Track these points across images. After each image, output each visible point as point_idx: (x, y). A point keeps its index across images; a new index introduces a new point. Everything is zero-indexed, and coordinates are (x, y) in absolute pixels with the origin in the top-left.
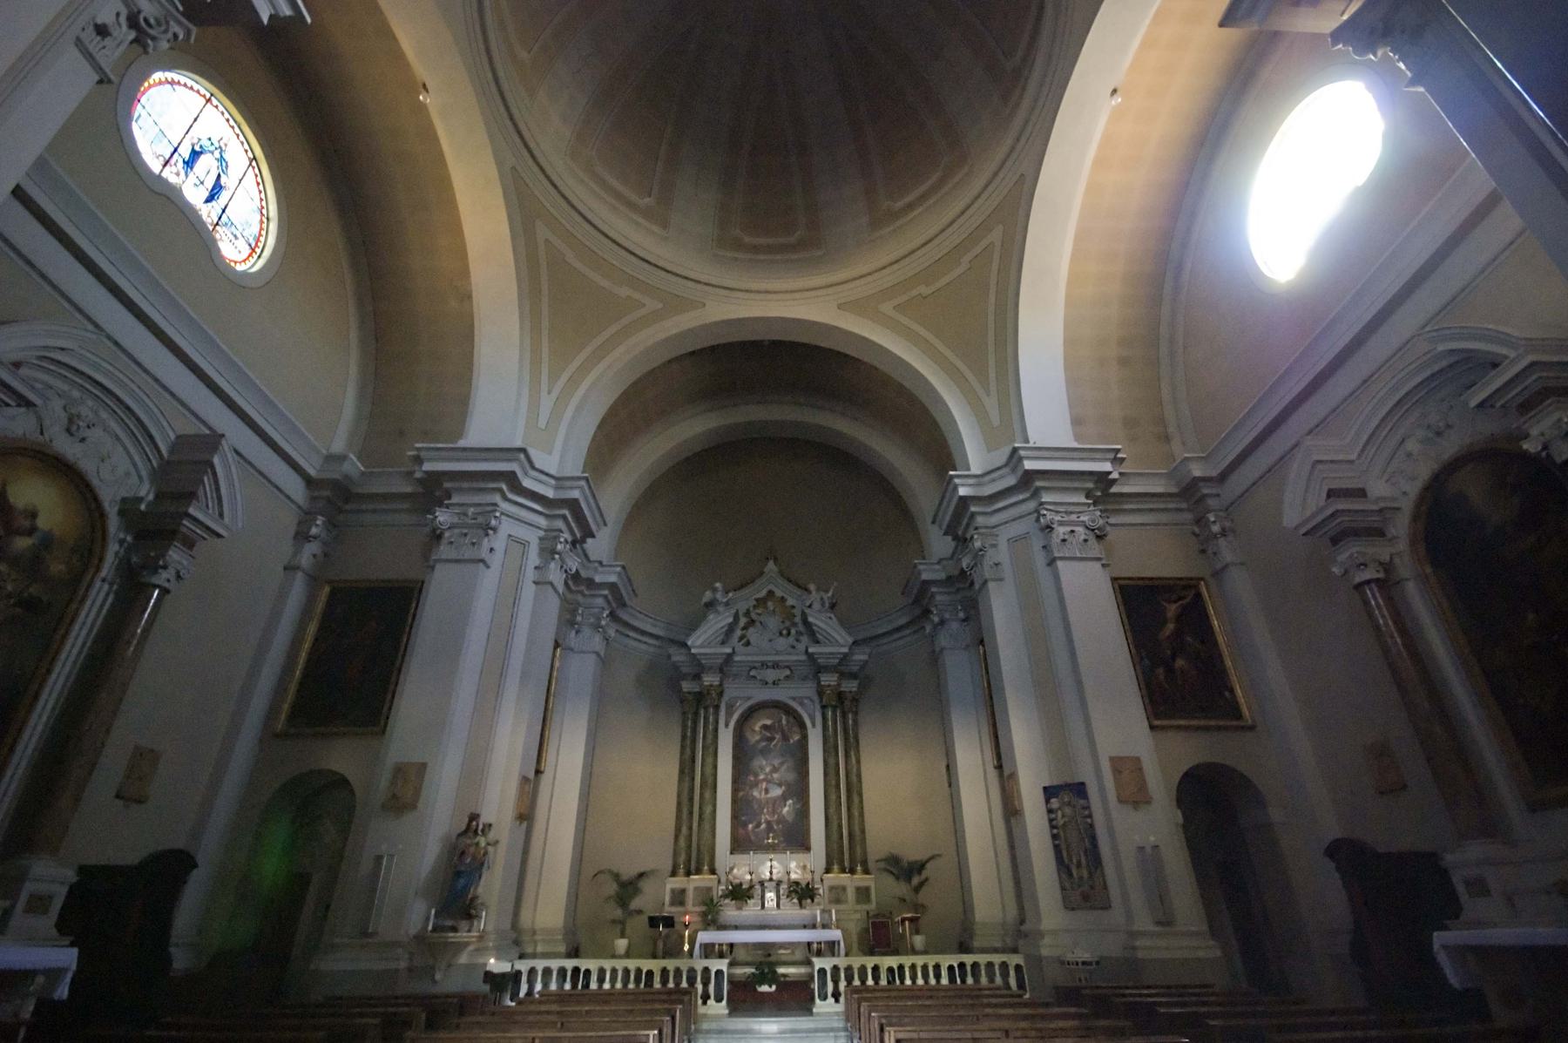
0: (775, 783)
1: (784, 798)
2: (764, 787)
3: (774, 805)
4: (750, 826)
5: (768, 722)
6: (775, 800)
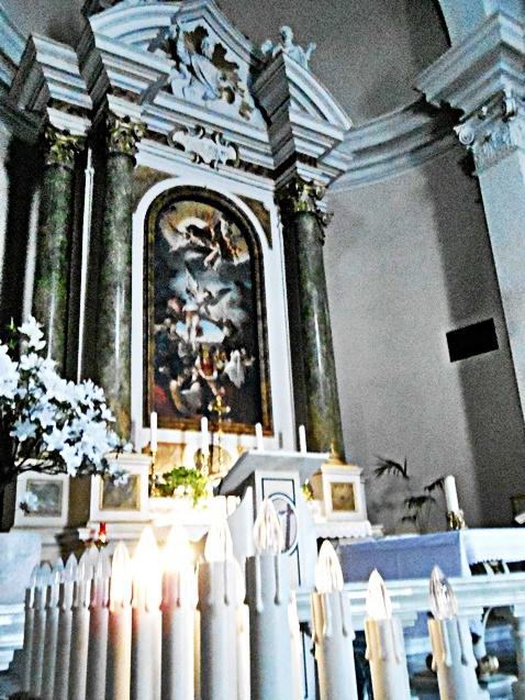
0: (213, 322)
1: (227, 347)
2: (194, 324)
3: (211, 357)
5: (201, 224)
6: (213, 348)
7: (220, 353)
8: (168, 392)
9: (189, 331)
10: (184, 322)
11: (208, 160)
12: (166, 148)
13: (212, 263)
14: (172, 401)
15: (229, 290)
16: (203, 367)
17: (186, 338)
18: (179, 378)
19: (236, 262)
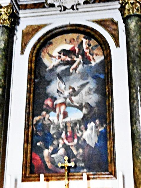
1: (85, 121)
2: (62, 111)
4: (46, 152)
5: (68, 47)
7: (80, 126)
8: (43, 158)
9: (58, 116)
10: (55, 111)
11: (69, 6)
12: (44, 10)
13: (75, 69)
14: (44, 163)
15: (87, 83)
16: (67, 138)
17: (56, 121)
18: (50, 147)
19: (93, 63)
